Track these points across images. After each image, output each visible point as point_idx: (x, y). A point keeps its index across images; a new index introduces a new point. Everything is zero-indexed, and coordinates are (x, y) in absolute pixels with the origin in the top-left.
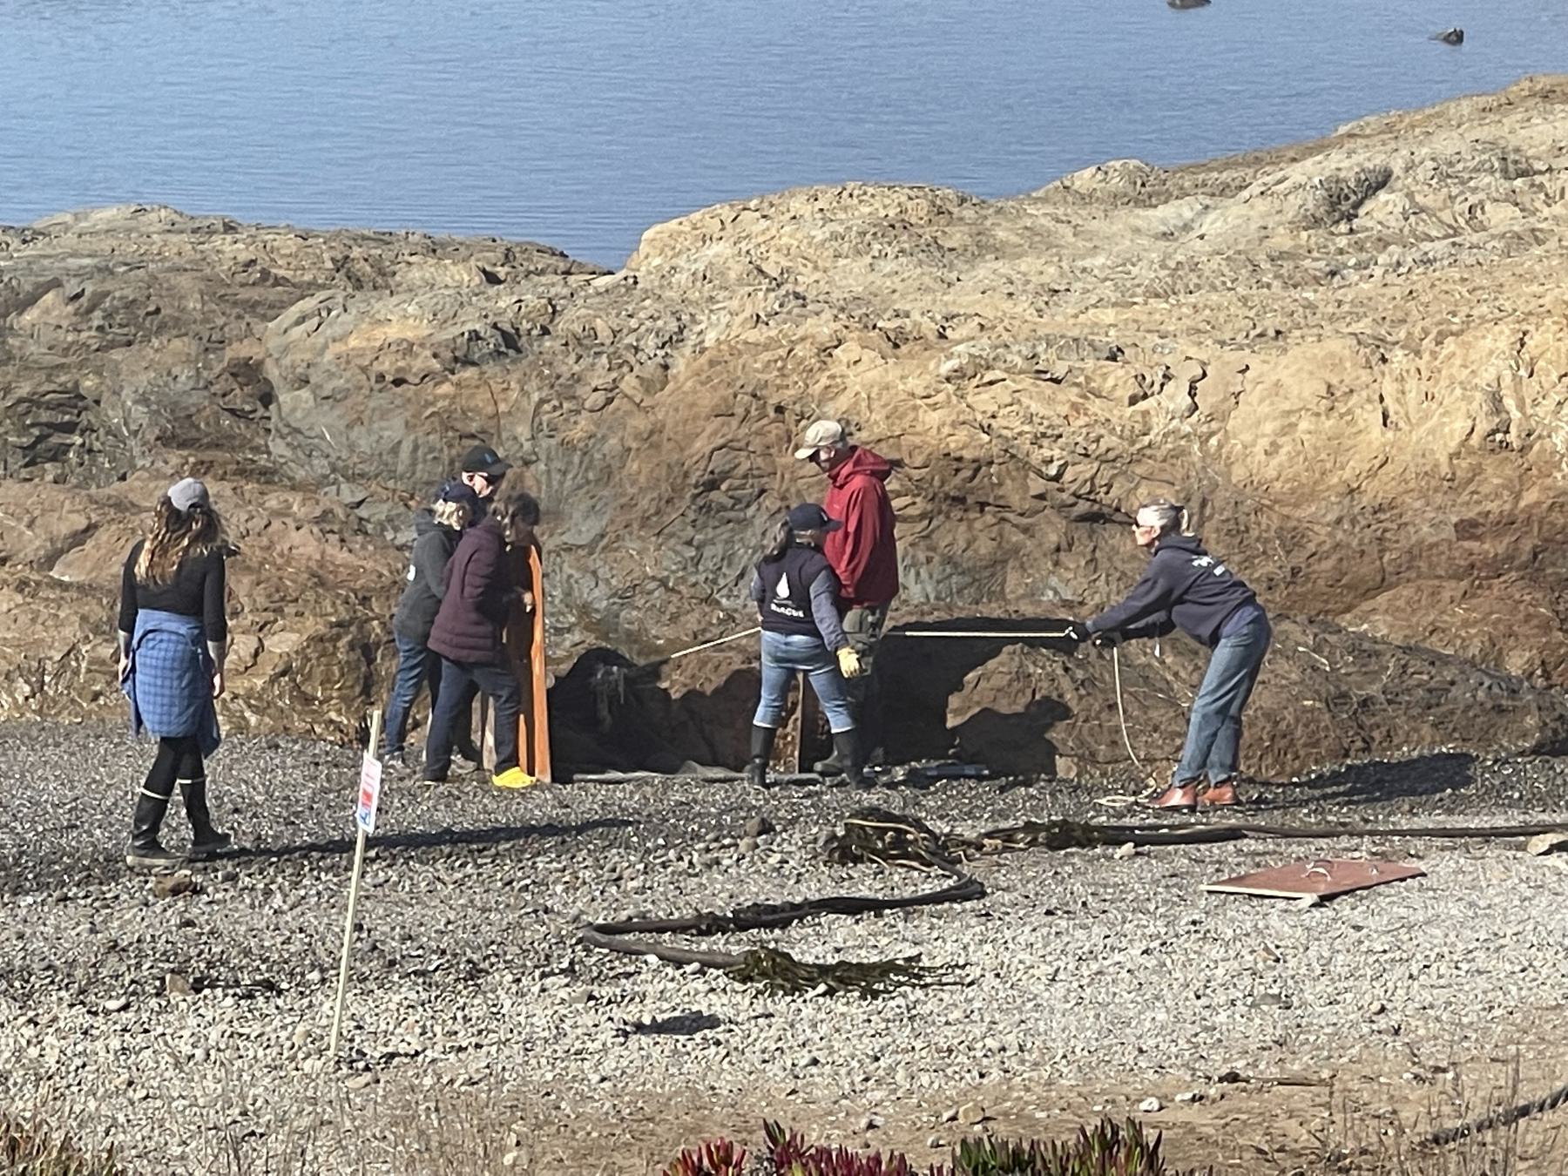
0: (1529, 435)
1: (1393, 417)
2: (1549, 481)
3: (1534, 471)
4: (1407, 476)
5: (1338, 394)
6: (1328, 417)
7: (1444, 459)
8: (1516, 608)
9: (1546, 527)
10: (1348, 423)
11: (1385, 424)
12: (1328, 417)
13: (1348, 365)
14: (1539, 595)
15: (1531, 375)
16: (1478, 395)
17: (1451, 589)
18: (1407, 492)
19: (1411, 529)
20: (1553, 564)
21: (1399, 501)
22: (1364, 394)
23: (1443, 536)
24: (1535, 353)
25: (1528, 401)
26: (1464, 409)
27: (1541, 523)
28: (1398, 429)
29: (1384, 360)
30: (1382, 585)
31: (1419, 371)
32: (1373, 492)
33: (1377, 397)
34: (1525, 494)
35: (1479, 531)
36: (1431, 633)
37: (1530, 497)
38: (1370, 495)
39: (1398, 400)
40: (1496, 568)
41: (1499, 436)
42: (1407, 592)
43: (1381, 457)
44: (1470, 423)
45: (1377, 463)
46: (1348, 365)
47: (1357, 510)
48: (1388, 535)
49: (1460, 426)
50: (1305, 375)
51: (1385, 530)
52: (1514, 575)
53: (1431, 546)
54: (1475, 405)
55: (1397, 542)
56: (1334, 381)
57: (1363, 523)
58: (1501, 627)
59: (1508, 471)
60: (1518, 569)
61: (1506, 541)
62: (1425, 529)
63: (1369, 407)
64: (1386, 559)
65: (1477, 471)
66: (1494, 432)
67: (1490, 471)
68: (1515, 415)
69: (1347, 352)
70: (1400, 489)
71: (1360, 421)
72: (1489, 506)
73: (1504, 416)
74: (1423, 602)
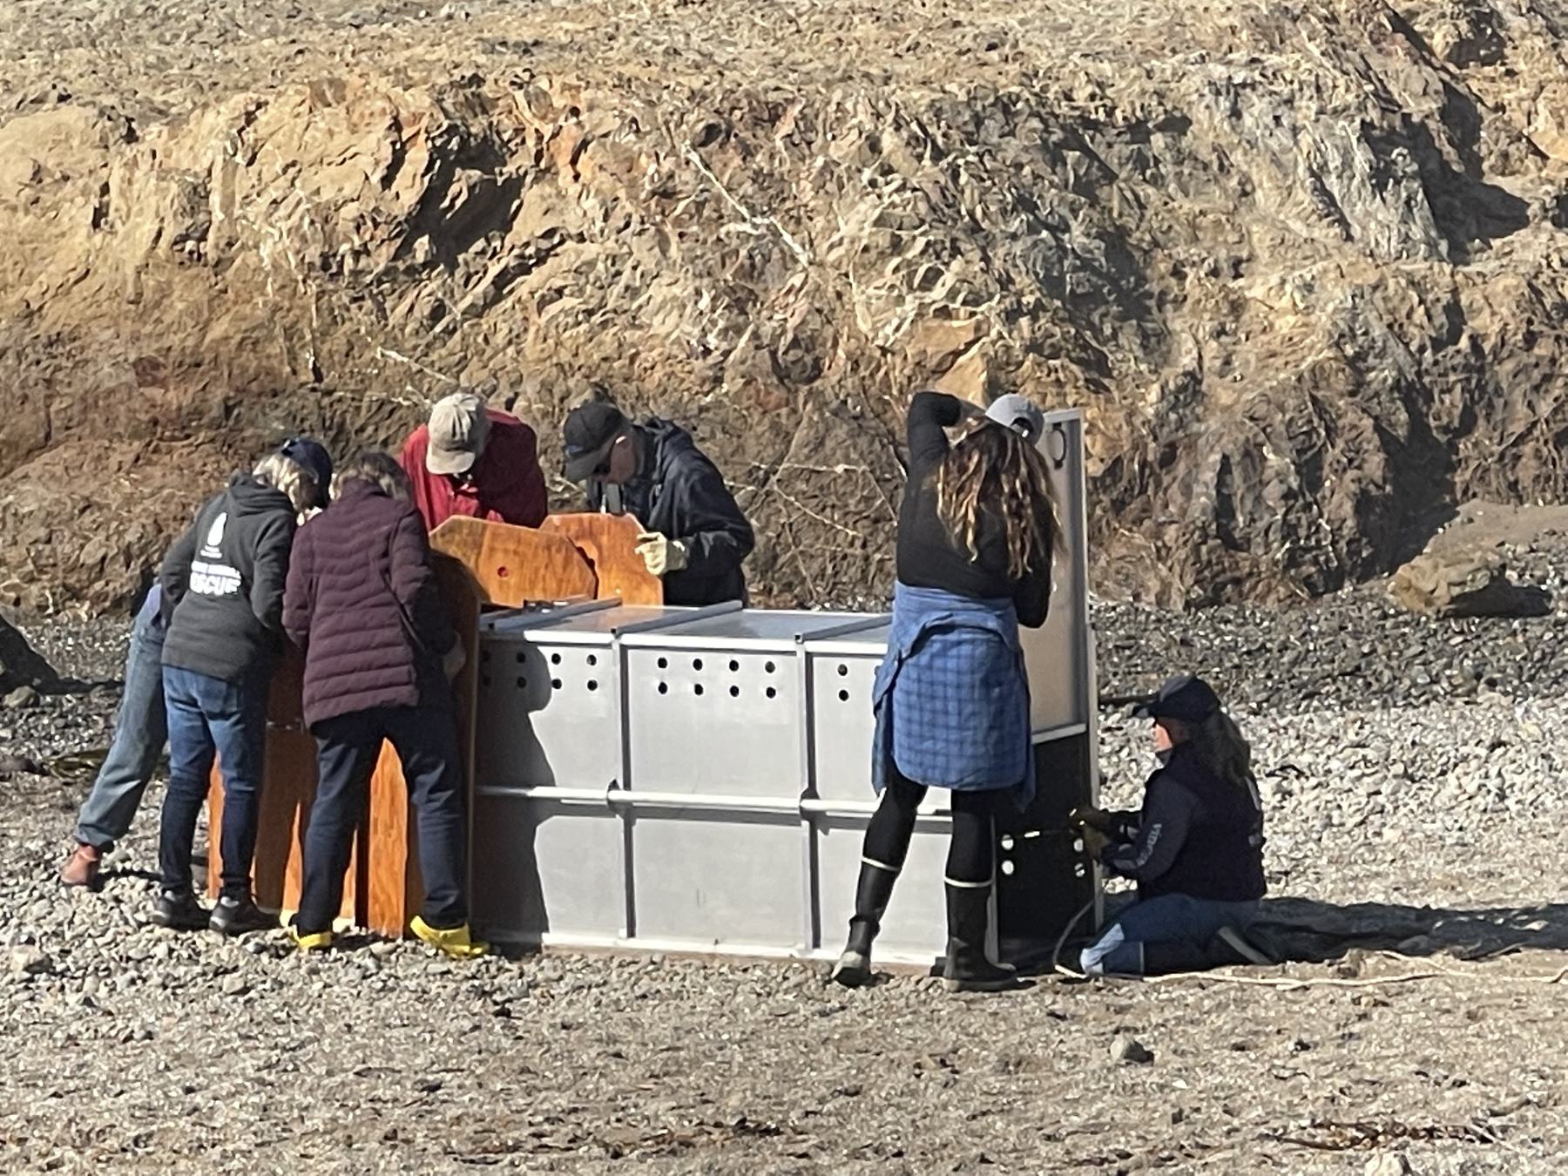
0: (230, 245)
1: (112, 215)
2: (248, 309)
3: (231, 294)
4: (103, 295)
5: (48, 180)
6: (27, 212)
7: (130, 271)
8: (195, 481)
9: (236, 371)
10: (49, 223)
11: (96, 224)
12: (27, 212)
13: (75, 142)
14: (225, 465)
15: (250, 163)
16: (174, 188)
17: (125, 451)
18: (95, 318)
19: (91, 368)
20: (252, 423)
21: (84, 330)
22: (80, 183)
23: (123, 379)
24: (263, 132)
25: (238, 198)
26: (153, 209)
27: (229, 365)
28: (113, 233)
29: (131, 137)
30: (46, 443)
31: (154, 154)
32: (56, 316)
33: (97, 188)
34: (214, 324)
35: (162, 373)
36: (83, 511)
37: (217, 330)
38: (50, 320)
39: (122, 193)
40: (184, 424)
41: (190, 245)
42: (66, 453)
43: (81, 270)
44: (156, 228)
45: (73, 276)
46: (75, 142)
47: (27, 340)
48: (60, 375)
49: (150, 227)
50: (13, 157)
51: (58, 368)
52: (202, 436)
53: (111, 392)
54: (168, 201)
55: (69, 384)
56: (50, 164)
57: (32, 357)
58: (172, 507)
59: (198, 293)
60: (209, 427)
61: (191, 391)
62: (107, 369)
63: (80, 200)
64: (53, 409)
65: (164, 291)
66: (184, 238)
67: (177, 293)
68: (218, 216)
69: (81, 125)
70: (88, 313)
71: (66, 219)
72: (174, 340)
73: (202, 217)
74: (85, 468)
